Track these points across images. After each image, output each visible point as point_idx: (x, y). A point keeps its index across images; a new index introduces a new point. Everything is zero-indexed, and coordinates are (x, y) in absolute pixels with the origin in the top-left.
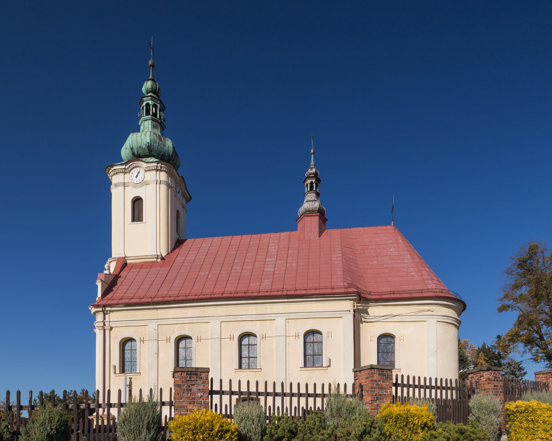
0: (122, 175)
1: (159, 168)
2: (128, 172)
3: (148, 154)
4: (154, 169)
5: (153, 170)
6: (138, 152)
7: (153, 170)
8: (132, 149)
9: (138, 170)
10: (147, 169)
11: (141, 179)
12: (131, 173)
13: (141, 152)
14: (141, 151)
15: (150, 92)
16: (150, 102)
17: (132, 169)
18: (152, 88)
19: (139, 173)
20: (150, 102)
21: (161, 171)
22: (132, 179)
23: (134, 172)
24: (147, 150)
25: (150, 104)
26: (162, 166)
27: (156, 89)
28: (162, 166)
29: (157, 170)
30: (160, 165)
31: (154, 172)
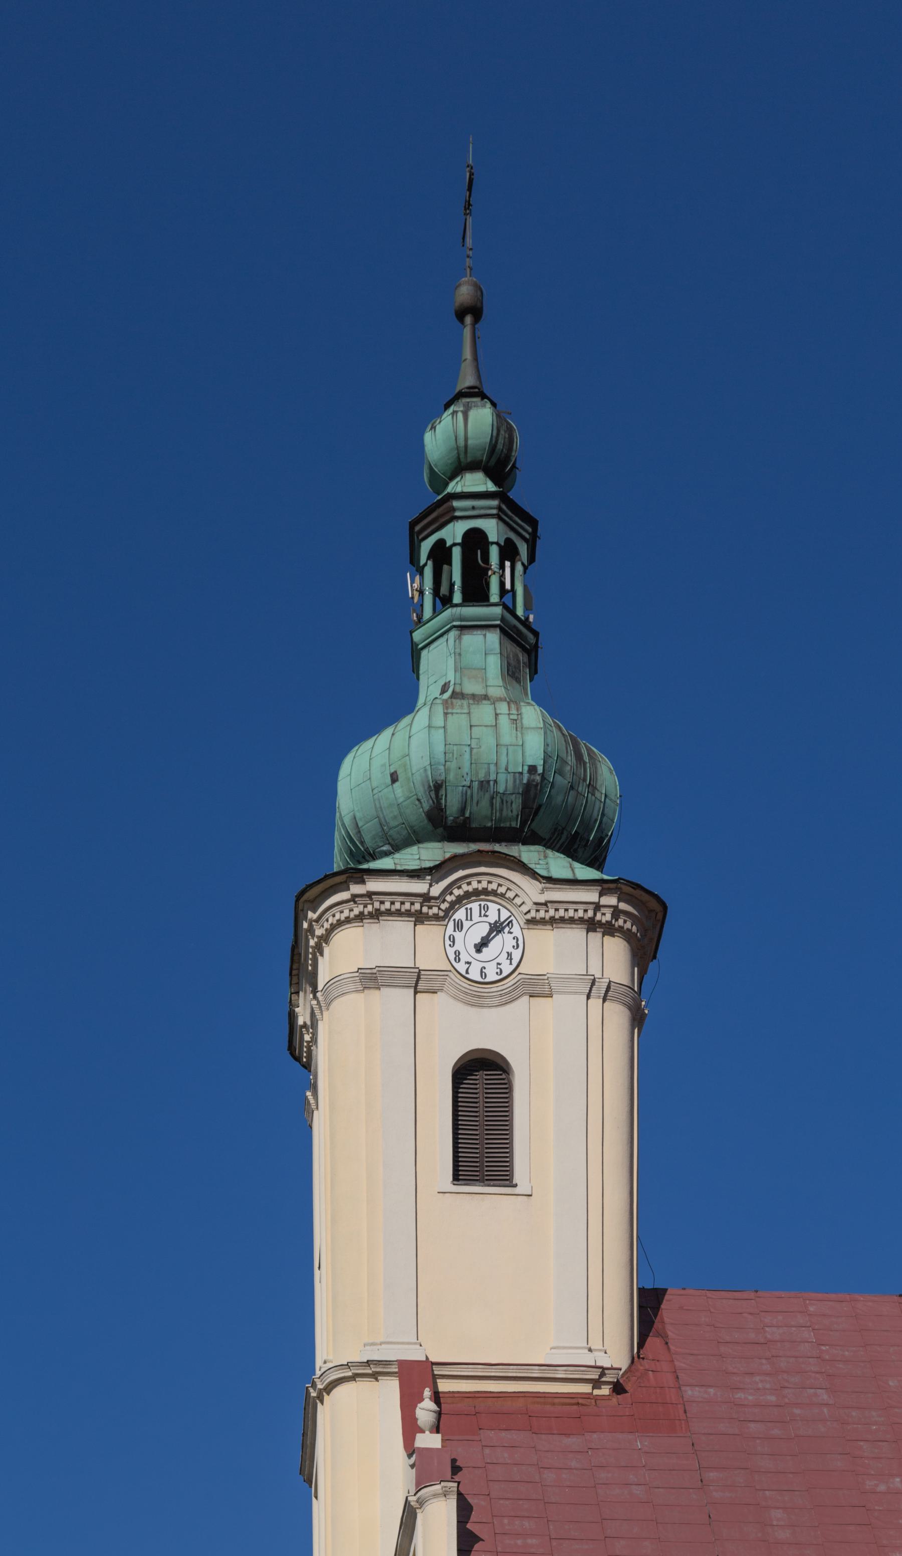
0: (404, 927)
1: (608, 917)
2: (436, 917)
3: (516, 824)
4: (581, 920)
5: (572, 921)
6: (463, 810)
7: (572, 921)
8: (437, 787)
9: (493, 917)
10: (542, 914)
11: (503, 958)
12: (451, 924)
13: (481, 811)
14: (485, 803)
15: (473, 467)
16: (492, 528)
17: (459, 901)
18: (493, 447)
19: (497, 928)
20: (492, 528)
21: (609, 930)
22: (457, 954)
23: (469, 916)
24: (517, 804)
25: (493, 537)
26: (623, 906)
27: (508, 457)
28: (623, 906)
29: (591, 925)
30: (612, 900)
31: (577, 934)
